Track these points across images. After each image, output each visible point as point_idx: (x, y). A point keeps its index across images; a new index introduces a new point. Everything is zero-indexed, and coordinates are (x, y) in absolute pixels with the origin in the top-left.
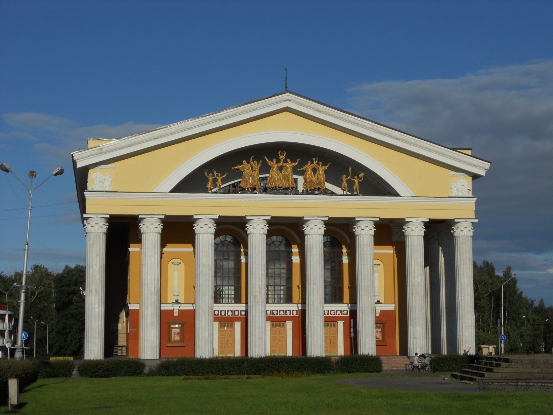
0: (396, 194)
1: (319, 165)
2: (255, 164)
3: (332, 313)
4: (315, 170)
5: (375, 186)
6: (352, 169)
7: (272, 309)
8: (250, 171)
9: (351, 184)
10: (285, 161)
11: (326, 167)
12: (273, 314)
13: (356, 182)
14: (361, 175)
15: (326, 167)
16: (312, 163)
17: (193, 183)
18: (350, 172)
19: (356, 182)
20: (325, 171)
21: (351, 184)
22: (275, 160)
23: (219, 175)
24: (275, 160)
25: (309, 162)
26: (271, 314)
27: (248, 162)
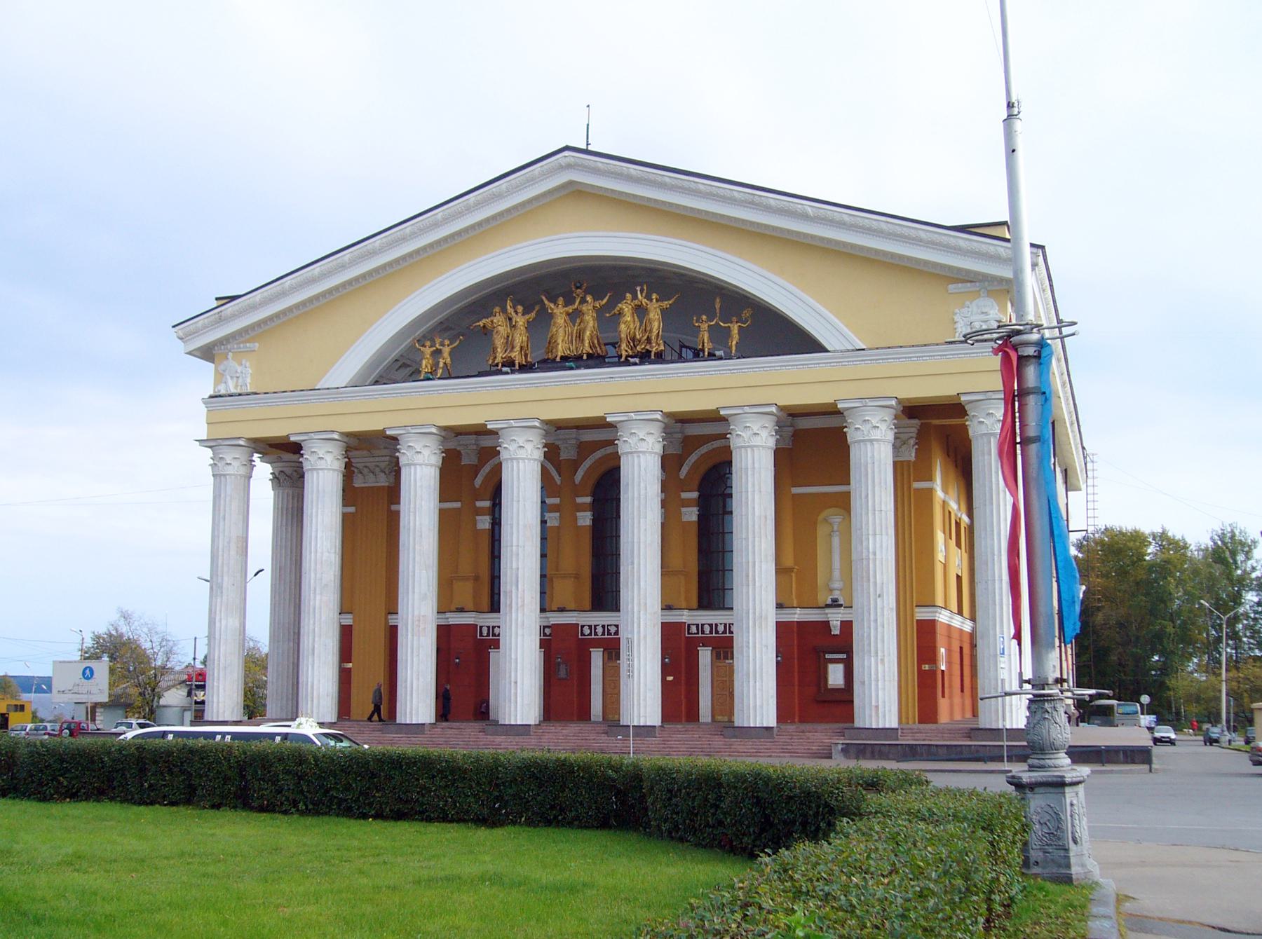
0: (823, 349)
1: (651, 300)
2: (516, 313)
3: (721, 629)
4: (640, 311)
5: (778, 335)
6: (721, 302)
7: (606, 624)
8: (510, 330)
9: (720, 336)
10: (583, 301)
11: (666, 304)
12: (609, 634)
13: (735, 331)
14: (746, 313)
15: (666, 304)
16: (635, 297)
17: (400, 366)
18: (718, 306)
19: (735, 331)
20: (664, 312)
21: (720, 336)
22: (561, 301)
23: (447, 342)
24: (561, 301)
25: (628, 296)
26: (603, 634)
27: (504, 310)
